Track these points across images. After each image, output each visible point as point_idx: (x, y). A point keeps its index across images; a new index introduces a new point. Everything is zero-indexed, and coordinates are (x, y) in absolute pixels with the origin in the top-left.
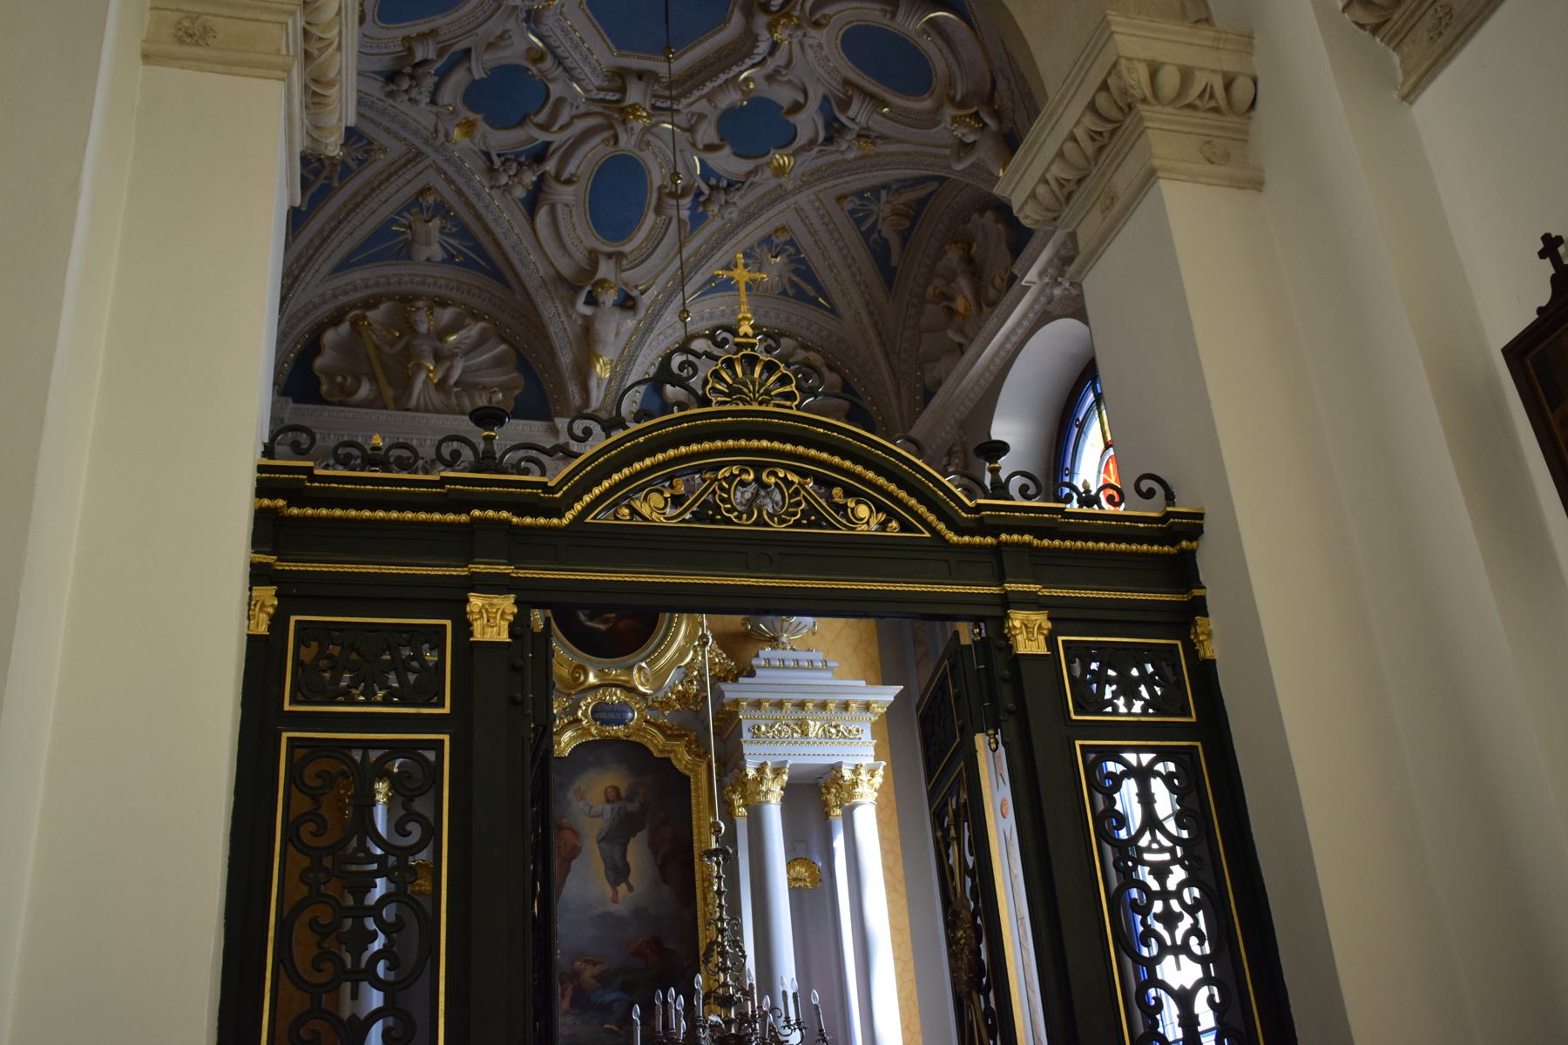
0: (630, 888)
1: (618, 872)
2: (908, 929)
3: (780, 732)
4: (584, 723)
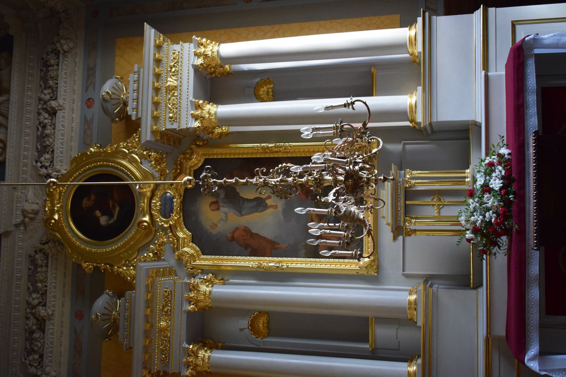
0: (269, 197)
2: (301, 23)
3: (173, 104)
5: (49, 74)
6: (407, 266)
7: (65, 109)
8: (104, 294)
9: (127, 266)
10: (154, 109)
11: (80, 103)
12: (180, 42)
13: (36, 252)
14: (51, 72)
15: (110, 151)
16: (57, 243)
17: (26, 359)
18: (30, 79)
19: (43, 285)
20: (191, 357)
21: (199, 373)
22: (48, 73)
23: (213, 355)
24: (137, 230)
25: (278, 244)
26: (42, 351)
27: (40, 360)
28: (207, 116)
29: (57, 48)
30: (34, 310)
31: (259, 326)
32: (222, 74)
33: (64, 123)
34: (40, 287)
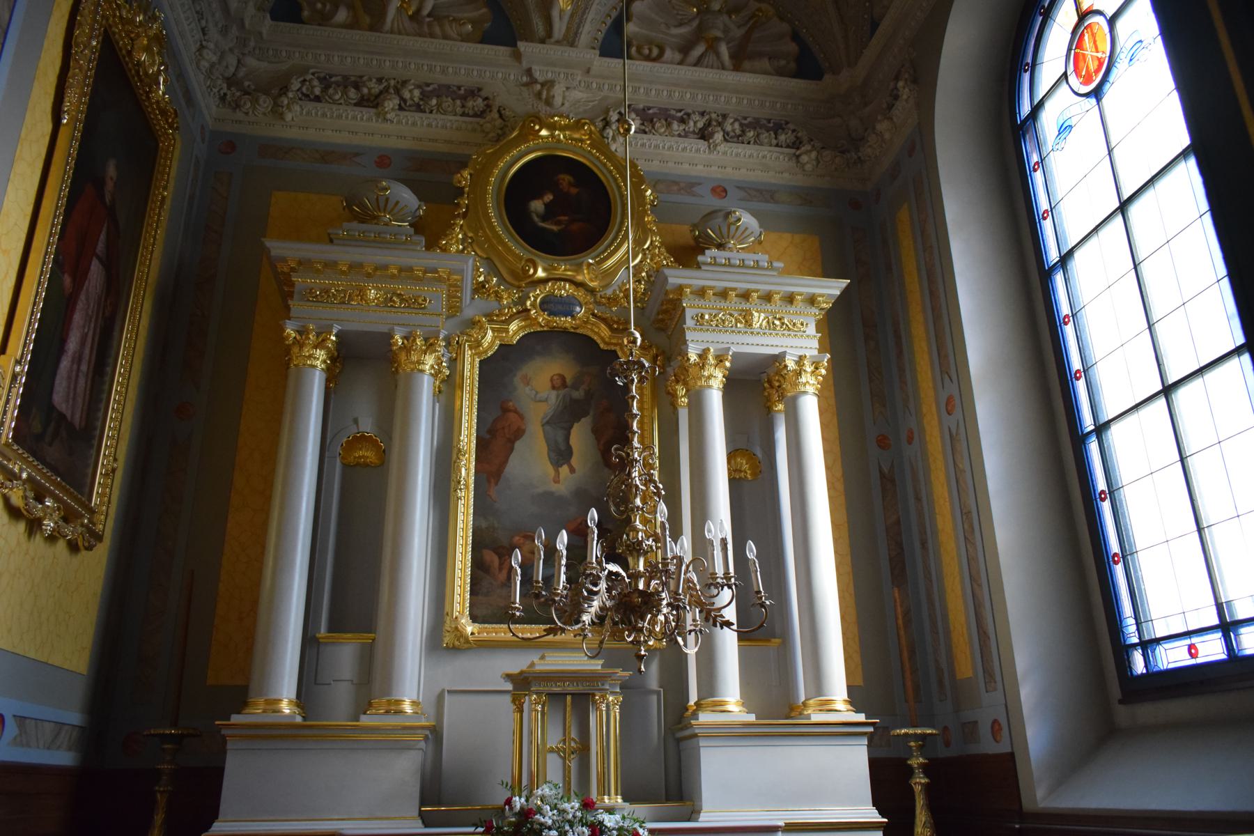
0: (572, 470)
1: (561, 455)
2: (846, 525)
3: (723, 321)
4: (532, 312)
5: (763, 131)
6: (456, 698)
7: (710, 153)
8: (419, 203)
9: (463, 241)
10: (716, 290)
11: (719, 176)
12: (820, 335)
13: (486, 99)
14: (767, 134)
15: (646, 219)
16: (500, 132)
17: (313, 74)
18: (757, 102)
19: (432, 107)
20: (315, 337)
21: (288, 350)
22: (765, 130)
23: (318, 373)
24: (521, 258)
25: (496, 484)
26: (327, 101)
27: (312, 97)
28: (706, 374)
29: (804, 146)
30: (393, 92)
31: (361, 449)
32: (768, 399)
33: (688, 150)
34: (430, 103)
